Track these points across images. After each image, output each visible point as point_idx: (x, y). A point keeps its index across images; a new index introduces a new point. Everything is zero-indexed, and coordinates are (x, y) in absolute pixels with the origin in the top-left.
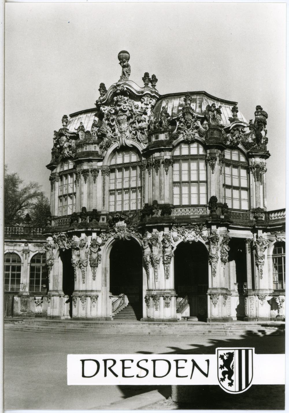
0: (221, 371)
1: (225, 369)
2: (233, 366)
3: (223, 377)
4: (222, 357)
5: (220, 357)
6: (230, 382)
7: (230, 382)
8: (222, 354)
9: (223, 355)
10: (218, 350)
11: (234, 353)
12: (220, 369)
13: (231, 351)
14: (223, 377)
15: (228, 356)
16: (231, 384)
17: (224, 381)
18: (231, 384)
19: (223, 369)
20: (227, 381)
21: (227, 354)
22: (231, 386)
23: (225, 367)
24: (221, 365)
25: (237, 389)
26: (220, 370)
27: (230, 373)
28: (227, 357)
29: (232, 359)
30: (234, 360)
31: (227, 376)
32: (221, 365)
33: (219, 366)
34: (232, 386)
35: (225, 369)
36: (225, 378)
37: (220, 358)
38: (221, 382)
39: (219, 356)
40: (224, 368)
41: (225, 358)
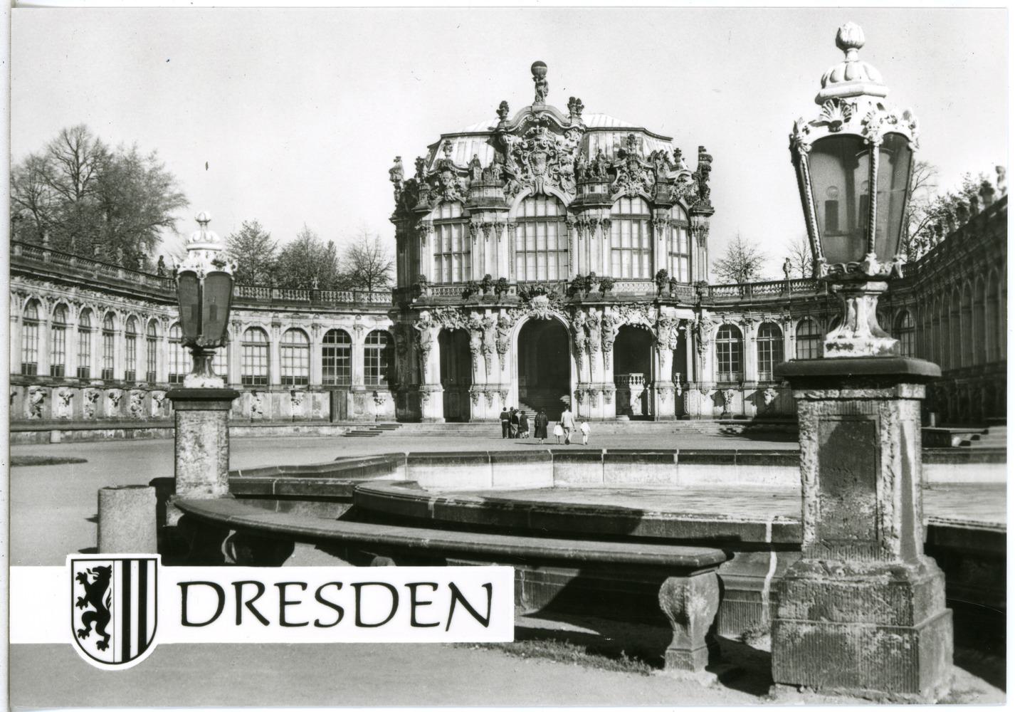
0: (79, 613)
1: (91, 608)
2: (108, 599)
3: (84, 628)
4: (82, 578)
5: (77, 579)
6: (101, 638)
7: (101, 638)
8: (83, 571)
9: (85, 574)
10: (73, 561)
11: (112, 569)
12: (79, 607)
13: (106, 564)
14: (84, 628)
15: (96, 574)
16: (102, 645)
17: (86, 637)
18: (102, 645)
19: (84, 607)
20: (94, 637)
21: (95, 570)
22: (104, 650)
23: (89, 603)
24: (80, 598)
25: (119, 658)
26: (77, 609)
27: (102, 617)
28: (94, 578)
29: (107, 584)
30: (111, 586)
31: (93, 624)
32: (80, 598)
33: (76, 601)
34: (106, 649)
35: (91, 608)
36: (89, 629)
37: (79, 581)
38: (81, 639)
39: (76, 575)
40: (87, 606)
41: (91, 580)
